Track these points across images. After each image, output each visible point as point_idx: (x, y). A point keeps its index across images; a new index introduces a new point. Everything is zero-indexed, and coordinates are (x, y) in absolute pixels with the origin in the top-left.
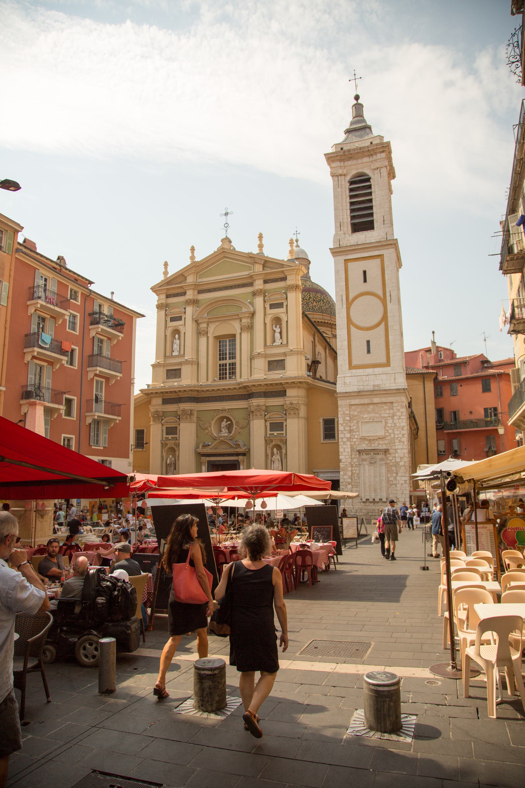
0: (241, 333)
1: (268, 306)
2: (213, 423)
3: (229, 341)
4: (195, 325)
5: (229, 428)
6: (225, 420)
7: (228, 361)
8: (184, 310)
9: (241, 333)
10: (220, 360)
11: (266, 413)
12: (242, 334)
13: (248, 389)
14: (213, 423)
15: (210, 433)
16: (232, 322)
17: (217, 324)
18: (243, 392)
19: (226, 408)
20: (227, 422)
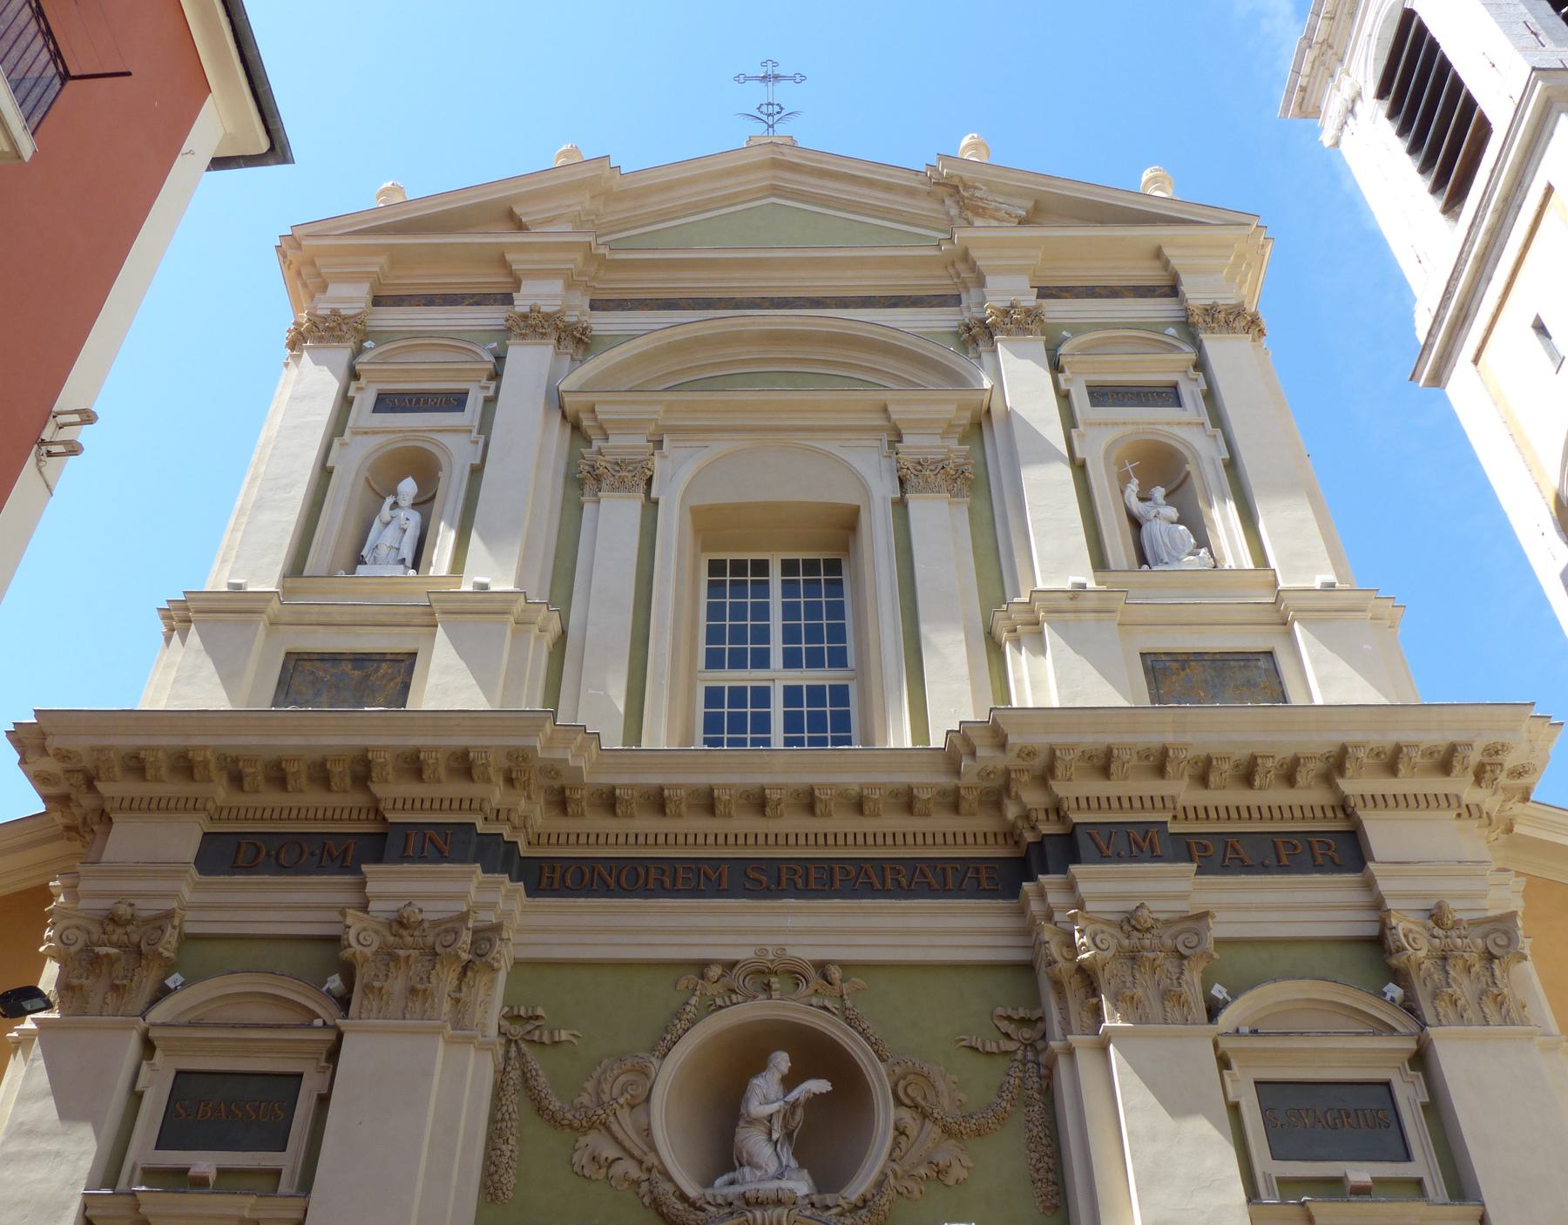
0: (901, 505)
1: (1080, 399)
2: (669, 1072)
3: (789, 567)
4: (558, 434)
5: (826, 1136)
6: (782, 1061)
7: (778, 677)
8: (489, 358)
9: (901, 505)
10: (714, 660)
11: (1219, 991)
12: (918, 506)
13: (1033, 798)
14: (669, 1072)
15: (629, 1168)
16: (831, 446)
17: (722, 446)
18: (968, 835)
19: (806, 951)
20: (789, 1082)
